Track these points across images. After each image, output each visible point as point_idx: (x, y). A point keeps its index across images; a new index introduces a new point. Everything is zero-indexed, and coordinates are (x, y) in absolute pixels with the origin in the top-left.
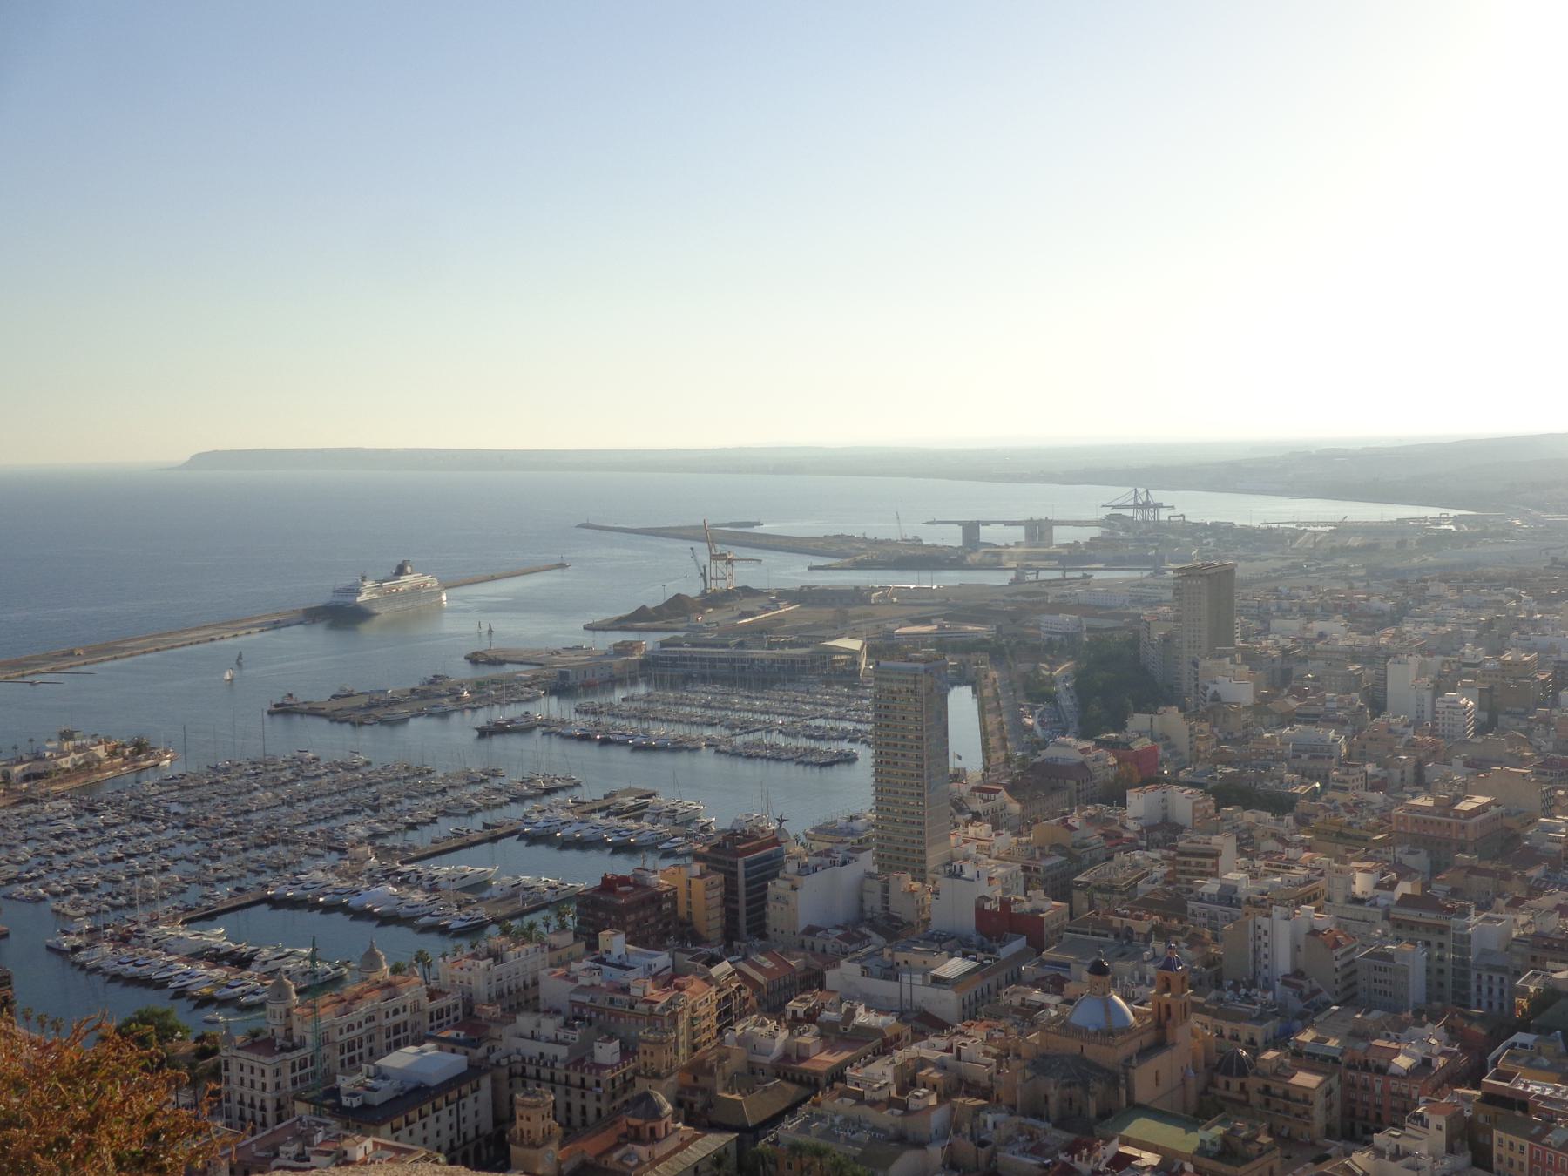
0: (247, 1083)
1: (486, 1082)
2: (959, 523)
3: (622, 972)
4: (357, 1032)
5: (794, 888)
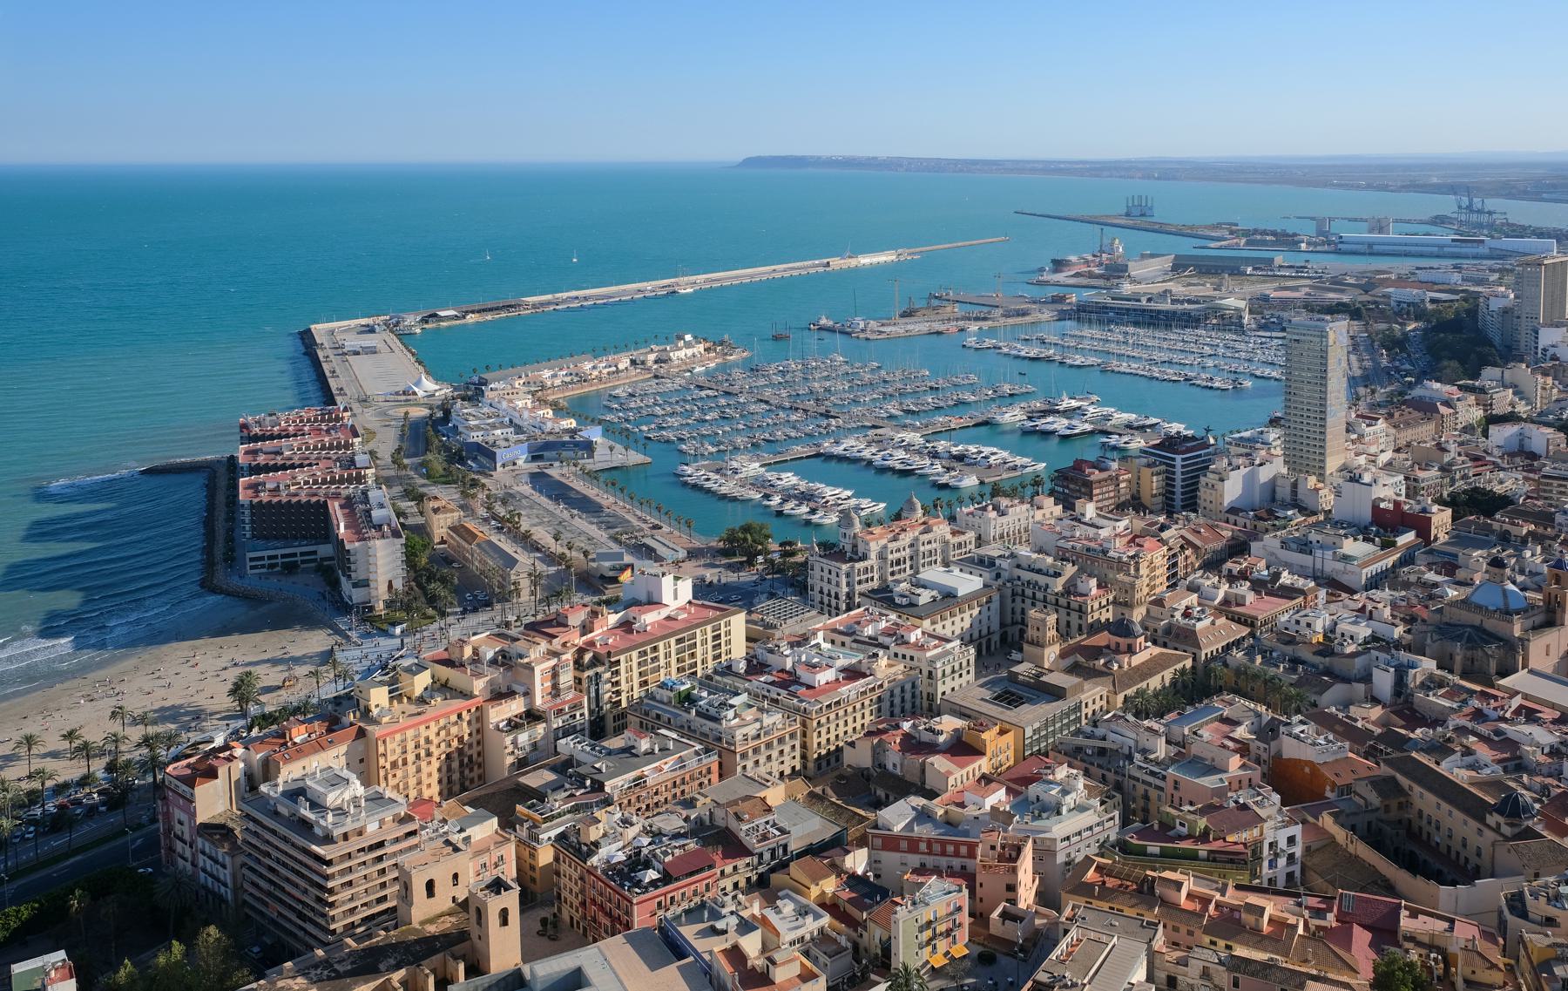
2: (1313, 219)
3: (1095, 530)
4: (903, 553)
5: (1222, 480)
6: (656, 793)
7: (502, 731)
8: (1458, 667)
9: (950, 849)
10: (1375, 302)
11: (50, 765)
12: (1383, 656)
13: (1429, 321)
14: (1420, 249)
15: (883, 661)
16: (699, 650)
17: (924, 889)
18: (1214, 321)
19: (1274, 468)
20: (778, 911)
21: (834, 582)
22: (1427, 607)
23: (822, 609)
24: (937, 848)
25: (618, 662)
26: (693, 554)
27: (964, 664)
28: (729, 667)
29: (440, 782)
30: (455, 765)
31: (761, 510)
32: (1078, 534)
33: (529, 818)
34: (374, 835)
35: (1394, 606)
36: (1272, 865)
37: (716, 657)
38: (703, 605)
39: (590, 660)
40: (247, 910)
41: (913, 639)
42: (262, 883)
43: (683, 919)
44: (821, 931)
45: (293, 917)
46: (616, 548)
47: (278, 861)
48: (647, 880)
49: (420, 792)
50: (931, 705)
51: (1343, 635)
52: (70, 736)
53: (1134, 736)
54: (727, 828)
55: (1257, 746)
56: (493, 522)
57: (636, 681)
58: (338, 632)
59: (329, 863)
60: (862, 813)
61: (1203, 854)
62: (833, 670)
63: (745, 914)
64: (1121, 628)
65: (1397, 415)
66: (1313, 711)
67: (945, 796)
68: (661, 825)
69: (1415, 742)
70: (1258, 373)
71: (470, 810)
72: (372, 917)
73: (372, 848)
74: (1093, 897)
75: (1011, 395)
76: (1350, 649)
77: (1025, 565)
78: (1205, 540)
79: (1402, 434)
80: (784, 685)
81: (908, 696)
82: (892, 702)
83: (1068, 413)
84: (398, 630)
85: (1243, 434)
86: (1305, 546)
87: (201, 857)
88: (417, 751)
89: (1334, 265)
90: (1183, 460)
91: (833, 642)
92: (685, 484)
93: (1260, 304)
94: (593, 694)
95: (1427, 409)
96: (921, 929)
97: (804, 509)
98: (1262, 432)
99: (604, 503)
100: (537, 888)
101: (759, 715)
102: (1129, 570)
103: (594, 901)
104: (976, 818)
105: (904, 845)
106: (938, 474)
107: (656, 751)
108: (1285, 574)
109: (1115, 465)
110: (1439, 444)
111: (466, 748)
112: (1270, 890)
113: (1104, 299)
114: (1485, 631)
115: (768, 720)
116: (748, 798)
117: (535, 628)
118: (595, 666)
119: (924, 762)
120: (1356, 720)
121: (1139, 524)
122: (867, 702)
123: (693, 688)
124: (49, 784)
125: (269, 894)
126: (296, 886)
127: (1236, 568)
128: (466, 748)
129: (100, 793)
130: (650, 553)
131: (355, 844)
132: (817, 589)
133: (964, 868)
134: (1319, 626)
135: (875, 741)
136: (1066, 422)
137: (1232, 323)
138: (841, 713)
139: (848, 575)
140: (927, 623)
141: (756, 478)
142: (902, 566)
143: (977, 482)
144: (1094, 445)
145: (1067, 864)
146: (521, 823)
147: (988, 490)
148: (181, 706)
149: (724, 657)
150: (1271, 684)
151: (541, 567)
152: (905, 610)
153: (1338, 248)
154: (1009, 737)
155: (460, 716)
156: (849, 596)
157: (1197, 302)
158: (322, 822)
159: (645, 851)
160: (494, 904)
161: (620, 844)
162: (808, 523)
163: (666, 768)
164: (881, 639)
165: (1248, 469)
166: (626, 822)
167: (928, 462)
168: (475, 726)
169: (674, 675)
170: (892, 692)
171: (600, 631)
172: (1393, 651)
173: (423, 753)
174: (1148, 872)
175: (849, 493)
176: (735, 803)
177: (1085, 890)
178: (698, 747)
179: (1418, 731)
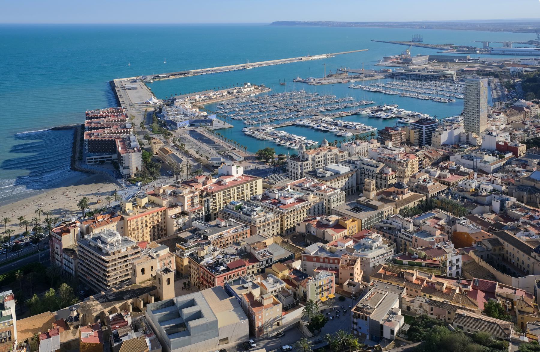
0: (293, 168)
2: (482, 42)
3: (392, 151)
4: (321, 159)
6: (227, 240)
7: (173, 218)
8: (525, 200)
9: (331, 261)
10: (504, 72)
11: (12, 228)
12: (496, 196)
13: (524, 78)
14: (522, 53)
15: (311, 196)
16: (245, 192)
17: (319, 275)
18: (443, 79)
19: (460, 130)
20: (267, 281)
21: (296, 169)
22: (514, 179)
23: (291, 178)
24: (326, 260)
25: (215, 195)
26: (246, 159)
27: (342, 197)
28: (255, 197)
29: (150, 235)
30: (156, 230)
31: (272, 144)
32: (385, 153)
33: (181, 248)
34: (124, 253)
35: (502, 179)
36: (451, 268)
37: (251, 194)
38: (247, 176)
39: (205, 195)
40: (79, 278)
41: (323, 188)
42: (85, 269)
43: (233, 283)
44: (283, 288)
45: (95, 281)
46: (219, 156)
47: (90, 261)
48: (221, 270)
49: (143, 239)
50: (329, 212)
51: (482, 189)
52: (20, 218)
53: (401, 223)
54: (251, 252)
55: (447, 227)
56: (175, 147)
57: (222, 202)
58: (118, 184)
59: (108, 262)
60: (301, 248)
61: (424, 264)
62: (293, 199)
63: (255, 282)
64: (399, 185)
65: (508, 112)
66: (469, 215)
67: (330, 243)
68: (227, 251)
69: (507, 227)
70: (458, 97)
71: (159, 245)
72: (124, 281)
73: (123, 257)
74: (381, 278)
75: (366, 104)
76: (484, 194)
77: (365, 163)
78: (433, 155)
79: (510, 118)
80: (275, 204)
81: (320, 208)
82: (314, 210)
83: (386, 111)
84: (139, 184)
85: (449, 118)
86: (470, 158)
87: (64, 260)
88: (142, 225)
89: (490, 59)
90: (426, 127)
91: (294, 189)
92: (245, 135)
93: (460, 73)
94: (206, 206)
95: (520, 109)
96: (318, 288)
97: (288, 143)
98: (456, 118)
99: (216, 141)
100: (183, 272)
101: (265, 214)
102: (404, 165)
103: (202, 277)
104: (341, 250)
105: (315, 259)
106: (337, 132)
107: (227, 226)
108: (462, 167)
109: (400, 129)
110: (523, 122)
111: (160, 224)
112: (450, 277)
113: (402, 71)
114: (536, 188)
115: (268, 216)
116: (258, 242)
117: (186, 183)
118: (207, 196)
119: (324, 231)
120: (485, 219)
121: (408, 149)
122: (305, 210)
123: (242, 204)
124: (12, 235)
125: (87, 273)
126: (96, 270)
127: (444, 165)
128: (160, 224)
129: (30, 238)
130: (231, 158)
131: (117, 256)
132: (290, 171)
133: (336, 268)
134: (473, 186)
135: (307, 224)
136: (385, 114)
137: (449, 79)
138: (295, 214)
139: (301, 166)
140: (329, 183)
141: (271, 133)
142: (321, 163)
143: (352, 135)
144: (395, 122)
145: (374, 267)
146: (178, 250)
147: (355, 137)
148: (62, 209)
149: (254, 194)
150: (455, 206)
151: (191, 163)
152: (321, 178)
153: (492, 53)
154: (356, 223)
155: (158, 213)
156: (301, 173)
157: (437, 72)
158: (106, 248)
159: (221, 260)
160: (165, 277)
161: (212, 257)
162: (289, 148)
163: (231, 232)
164: (311, 188)
165: (450, 130)
166: (215, 250)
167: (334, 127)
168: (163, 217)
169: (236, 200)
170: (314, 208)
171: (209, 185)
172: (500, 194)
173: (144, 226)
174: (402, 270)
175: (305, 138)
176: (254, 244)
177: (378, 276)
178: (243, 225)
179: (509, 223)
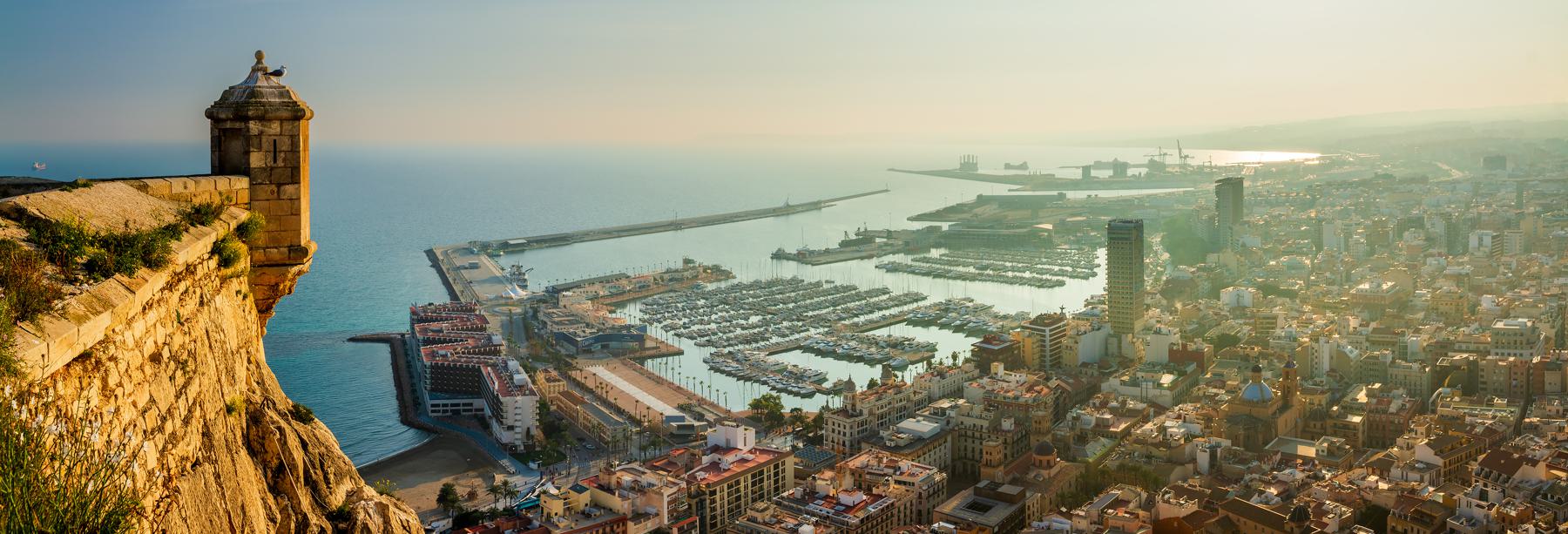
0: (836, 431)
1: (949, 438)
4: (885, 409)
90: (1051, 331)
